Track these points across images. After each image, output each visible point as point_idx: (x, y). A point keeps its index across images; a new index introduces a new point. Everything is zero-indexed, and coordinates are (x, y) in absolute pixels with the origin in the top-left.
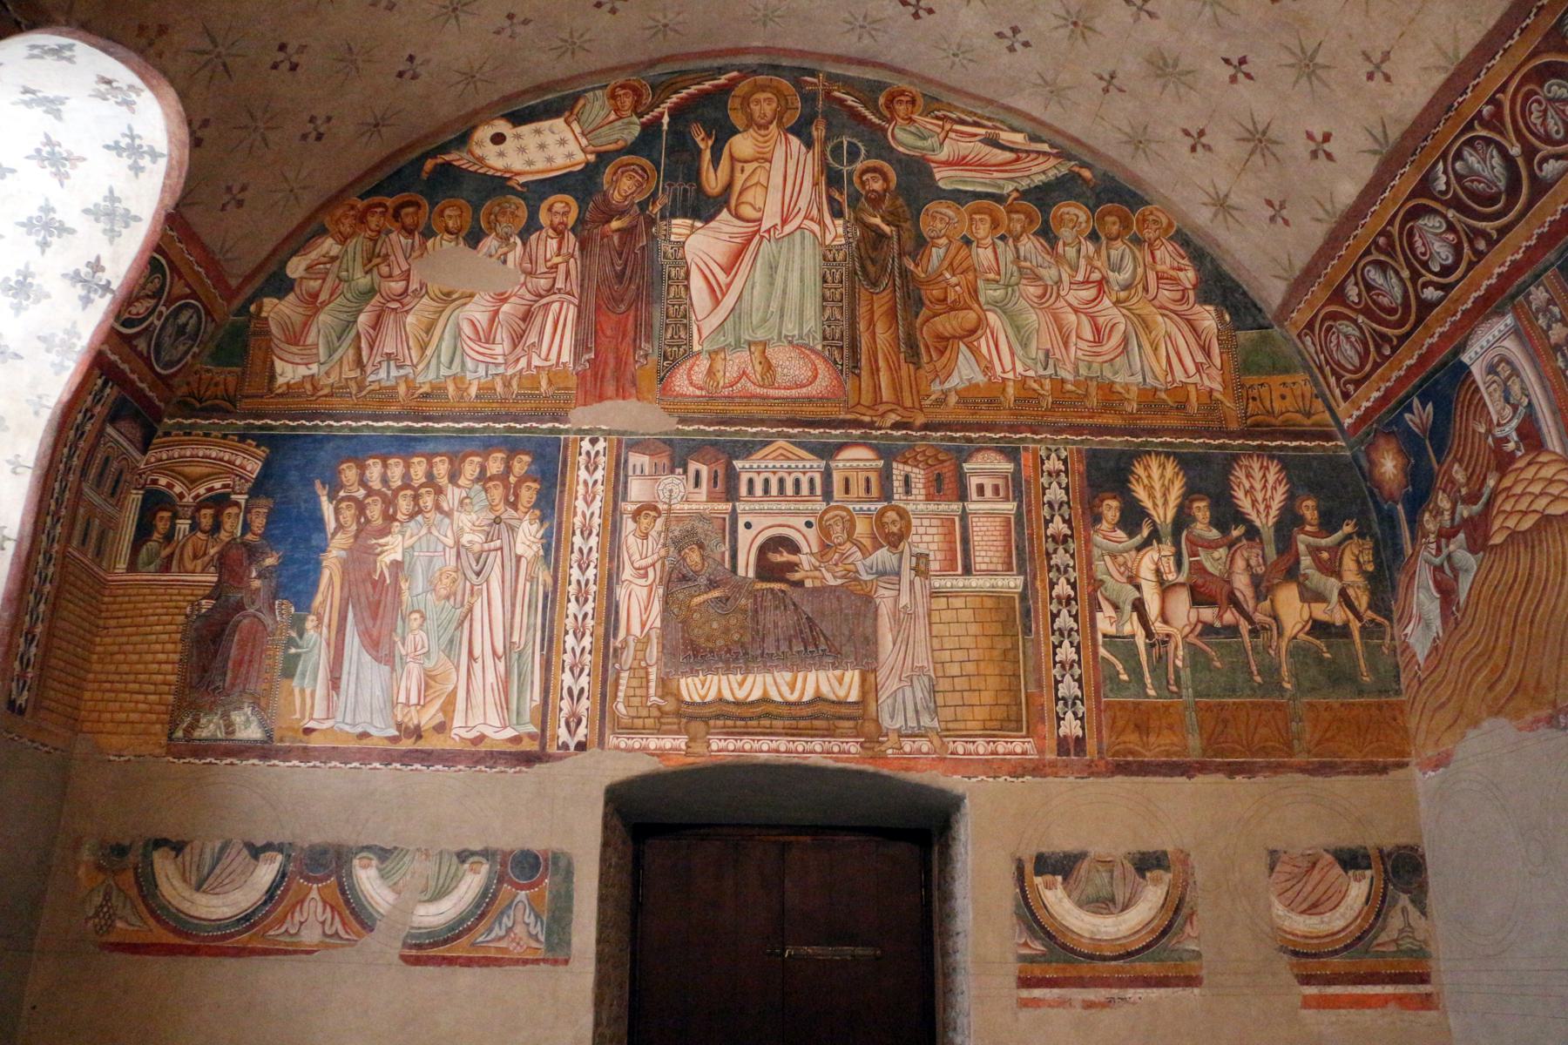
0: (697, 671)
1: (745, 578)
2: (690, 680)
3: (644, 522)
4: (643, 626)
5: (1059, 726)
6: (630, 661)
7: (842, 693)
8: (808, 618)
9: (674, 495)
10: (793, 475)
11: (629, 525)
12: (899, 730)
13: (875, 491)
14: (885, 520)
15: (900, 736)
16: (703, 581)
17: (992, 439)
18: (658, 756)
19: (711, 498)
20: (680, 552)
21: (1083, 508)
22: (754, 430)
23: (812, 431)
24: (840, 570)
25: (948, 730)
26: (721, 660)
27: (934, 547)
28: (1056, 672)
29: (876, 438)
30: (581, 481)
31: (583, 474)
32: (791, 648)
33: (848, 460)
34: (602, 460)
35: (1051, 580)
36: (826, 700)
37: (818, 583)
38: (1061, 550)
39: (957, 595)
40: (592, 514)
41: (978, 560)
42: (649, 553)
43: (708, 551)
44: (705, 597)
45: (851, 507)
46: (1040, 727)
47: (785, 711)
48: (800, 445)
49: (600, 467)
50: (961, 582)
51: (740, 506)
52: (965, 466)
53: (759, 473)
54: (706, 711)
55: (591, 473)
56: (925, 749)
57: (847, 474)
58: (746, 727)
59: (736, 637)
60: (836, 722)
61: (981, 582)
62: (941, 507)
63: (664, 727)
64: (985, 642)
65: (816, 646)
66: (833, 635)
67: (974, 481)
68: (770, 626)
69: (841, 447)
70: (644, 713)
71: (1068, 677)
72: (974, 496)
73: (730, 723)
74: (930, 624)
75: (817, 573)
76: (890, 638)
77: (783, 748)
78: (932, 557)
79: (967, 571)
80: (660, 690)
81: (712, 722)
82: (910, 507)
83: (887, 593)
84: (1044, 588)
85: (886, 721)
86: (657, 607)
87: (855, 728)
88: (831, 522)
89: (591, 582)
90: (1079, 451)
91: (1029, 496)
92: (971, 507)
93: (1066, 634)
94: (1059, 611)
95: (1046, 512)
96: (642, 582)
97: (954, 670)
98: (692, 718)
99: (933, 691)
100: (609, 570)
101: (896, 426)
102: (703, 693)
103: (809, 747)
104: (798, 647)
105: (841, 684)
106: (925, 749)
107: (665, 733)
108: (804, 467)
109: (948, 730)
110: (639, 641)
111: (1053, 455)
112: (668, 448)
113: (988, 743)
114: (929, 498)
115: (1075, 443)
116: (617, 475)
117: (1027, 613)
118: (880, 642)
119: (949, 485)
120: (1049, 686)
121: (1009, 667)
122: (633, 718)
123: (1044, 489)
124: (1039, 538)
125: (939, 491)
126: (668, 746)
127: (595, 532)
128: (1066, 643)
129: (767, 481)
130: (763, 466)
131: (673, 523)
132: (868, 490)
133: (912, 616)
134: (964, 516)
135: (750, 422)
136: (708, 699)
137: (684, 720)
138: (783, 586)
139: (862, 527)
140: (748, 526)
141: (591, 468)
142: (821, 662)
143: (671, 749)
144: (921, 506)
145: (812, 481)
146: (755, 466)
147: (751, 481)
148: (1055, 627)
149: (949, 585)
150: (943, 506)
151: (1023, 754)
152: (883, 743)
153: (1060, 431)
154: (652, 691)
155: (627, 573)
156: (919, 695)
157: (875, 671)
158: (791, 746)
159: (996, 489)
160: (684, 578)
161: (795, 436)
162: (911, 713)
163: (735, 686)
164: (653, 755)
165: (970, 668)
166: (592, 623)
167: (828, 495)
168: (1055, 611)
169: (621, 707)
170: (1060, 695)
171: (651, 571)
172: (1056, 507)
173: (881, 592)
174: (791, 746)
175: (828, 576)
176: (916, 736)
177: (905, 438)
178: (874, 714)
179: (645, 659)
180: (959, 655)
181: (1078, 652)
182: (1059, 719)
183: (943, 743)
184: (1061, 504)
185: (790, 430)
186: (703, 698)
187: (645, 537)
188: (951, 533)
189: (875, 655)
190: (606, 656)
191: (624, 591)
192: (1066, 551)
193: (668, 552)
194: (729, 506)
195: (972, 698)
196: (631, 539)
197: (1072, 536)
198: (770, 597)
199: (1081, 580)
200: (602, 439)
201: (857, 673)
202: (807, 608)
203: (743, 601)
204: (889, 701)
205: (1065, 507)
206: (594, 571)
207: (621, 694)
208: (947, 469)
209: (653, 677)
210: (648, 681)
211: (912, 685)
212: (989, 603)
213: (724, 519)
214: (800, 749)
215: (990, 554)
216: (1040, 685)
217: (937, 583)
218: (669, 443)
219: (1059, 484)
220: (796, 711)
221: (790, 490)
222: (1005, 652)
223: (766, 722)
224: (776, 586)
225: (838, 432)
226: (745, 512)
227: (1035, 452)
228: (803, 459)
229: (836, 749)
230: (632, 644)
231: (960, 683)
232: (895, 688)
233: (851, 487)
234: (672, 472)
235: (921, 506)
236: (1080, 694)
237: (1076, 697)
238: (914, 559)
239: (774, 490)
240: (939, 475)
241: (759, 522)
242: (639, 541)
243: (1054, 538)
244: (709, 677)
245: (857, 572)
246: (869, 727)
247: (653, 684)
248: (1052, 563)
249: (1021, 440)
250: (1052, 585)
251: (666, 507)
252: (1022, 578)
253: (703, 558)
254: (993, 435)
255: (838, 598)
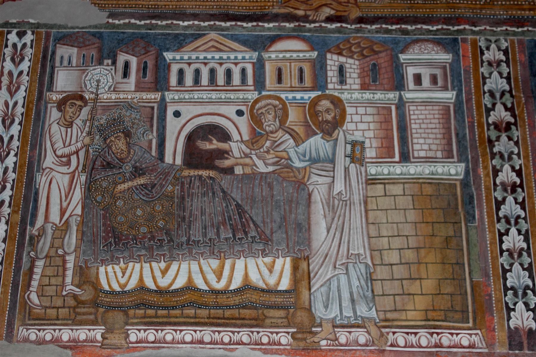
0: (118, 258)
1: (174, 164)
2: (109, 269)
3: (70, 111)
4: (63, 213)
5: (509, 318)
6: (46, 249)
7: (272, 281)
8: (238, 206)
9: (102, 85)
10: (225, 66)
11: (54, 114)
12: (333, 320)
13: (308, 82)
14: (319, 108)
15: (334, 327)
16: (128, 168)
17: (429, 32)
18: (71, 348)
19: (139, 88)
20: (105, 140)
21: (527, 98)
22: (186, 23)
23: (245, 25)
24: (271, 158)
25: (386, 320)
26: (144, 248)
27: (371, 134)
28: (504, 260)
29: (310, 30)
30: (6, 72)
31: (8, 65)
32: (218, 234)
33: (281, 51)
34: (29, 52)
35: (494, 167)
36: (256, 289)
37: (248, 170)
38: (504, 138)
39: (394, 182)
40: (16, 103)
41: (416, 147)
42: (73, 141)
43: (134, 140)
44: (130, 184)
45: (283, 96)
46: (487, 317)
47: (211, 300)
48: (234, 38)
49: (27, 59)
50: (398, 169)
51: (169, 96)
52: (402, 57)
53: (189, 64)
54: (126, 300)
55: (17, 64)
56: (362, 340)
57: (280, 65)
58: (169, 316)
59: (161, 224)
60: (265, 311)
61: (419, 169)
62: (377, 96)
63: (79, 318)
64: (429, 229)
65: (246, 233)
66: (264, 222)
67: (411, 71)
68: (198, 213)
69: (274, 39)
70: (59, 303)
71: (516, 266)
72: (411, 85)
73: (150, 312)
74: (366, 211)
75: (247, 161)
76: (323, 225)
77: (207, 339)
78: (367, 144)
79: (405, 157)
80: (77, 279)
81: (131, 312)
82: (345, 96)
83: (321, 180)
84: (487, 175)
85: (319, 311)
86: (78, 195)
87: (286, 318)
88: (263, 110)
89: (11, 169)
90: (520, 42)
91: (468, 82)
92: (408, 95)
93: (513, 221)
94: (504, 199)
95: (487, 100)
96: (64, 169)
97: (393, 257)
98: (111, 308)
99: (371, 278)
100: (30, 157)
101: (329, 19)
102: (123, 281)
103: (236, 338)
104: (226, 233)
105: (271, 271)
106: (362, 340)
107: (81, 323)
108: (236, 58)
109: (386, 320)
110: (57, 228)
111: (493, 46)
112: (96, 40)
113: (432, 334)
114: (364, 87)
115: (515, 34)
116: (44, 66)
117: (469, 200)
118: (313, 227)
119: (385, 76)
120: (496, 275)
121: (451, 254)
122: (46, 308)
123: (484, 78)
124: (481, 125)
125: (374, 81)
126: (83, 337)
127: (17, 121)
128: (513, 231)
129: (197, 72)
130: (194, 57)
131: (99, 112)
132: (301, 79)
133: (348, 204)
134: (401, 105)
135: (183, 16)
136: (128, 288)
137: (101, 310)
138: (212, 173)
139: (293, 116)
140: (177, 114)
141: (17, 60)
142: (250, 249)
143: (85, 341)
144: (356, 95)
145: (243, 71)
146: (186, 57)
147: (181, 72)
148: (501, 214)
149: (386, 171)
150: (379, 95)
151: (470, 347)
152: (316, 333)
153: (498, 23)
154: (69, 280)
155: (49, 161)
156: (355, 283)
157: (307, 258)
158: (217, 336)
159: (434, 79)
160: (109, 165)
161: (227, 29)
162: (346, 303)
163: (158, 274)
164: (65, 347)
165: (410, 255)
166: (9, 210)
167: (259, 84)
168: (500, 199)
169: (34, 297)
170: (509, 285)
171: (74, 159)
172: (498, 96)
173: (314, 178)
174: (217, 336)
175: (259, 163)
176: (353, 326)
177: (338, 30)
178: (307, 303)
179: (62, 247)
180: (397, 243)
181: (526, 240)
182: (509, 310)
183: (382, 335)
184: (503, 94)
185: (223, 24)
186: (123, 286)
187: (70, 125)
188: (388, 121)
189: (308, 241)
190: (21, 246)
191: (44, 179)
192: (510, 139)
193: (92, 140)
194: (157, 96)
195: (415, 288)
196: (55, 128)
197: (515, 124)
198: (197, 183)
199: (527, 167)
200: (29, 32)
201: (288, 259)
202: (236, 195)
203: (170, 188)
204: (323, 289)
205: (507, 95)
206: (15, 159)
207: (35, 284)
208: (383, 59)
209: (70, 265)
210: (65, 270)
211: (347, 273)
212: (428, 190)
213: (153, 108)
214: (226, 340)
215: (430, 141)
216: (487, 275)
217: (373, 170)
218: (99, 36)
219: (500, 74)
220: (222, 300)
221: (221, 79)
222: (447, 240)
223: (191, 312)
224: (205, 173)
225: (271, 25)
226: (174, 102)
227: (474, 43)
228: (235, 51)
229: (265, 340)
230: (50, 232)
231: (399, 272)
232: (329, 276)
233: (284, 77)
234: (100, 63)
235: (356, 95)
236: (531, 284)
237: (527, 287)
238: (349, 147)
239: (205, 80)
240: (374, 65)
241: (188, 111)
242: (63, 129)
243: (497, 126)
244: (131, 265)
245: (290, 159)
246: (301, 316)
247: (69, 273)
248: (495, 150)
249: (458, 31)
250: (496, 172)
251: (92, 96)
252: (463, 165)
253: (128, 144)
254: (430, 28)
255: (270, 186)
